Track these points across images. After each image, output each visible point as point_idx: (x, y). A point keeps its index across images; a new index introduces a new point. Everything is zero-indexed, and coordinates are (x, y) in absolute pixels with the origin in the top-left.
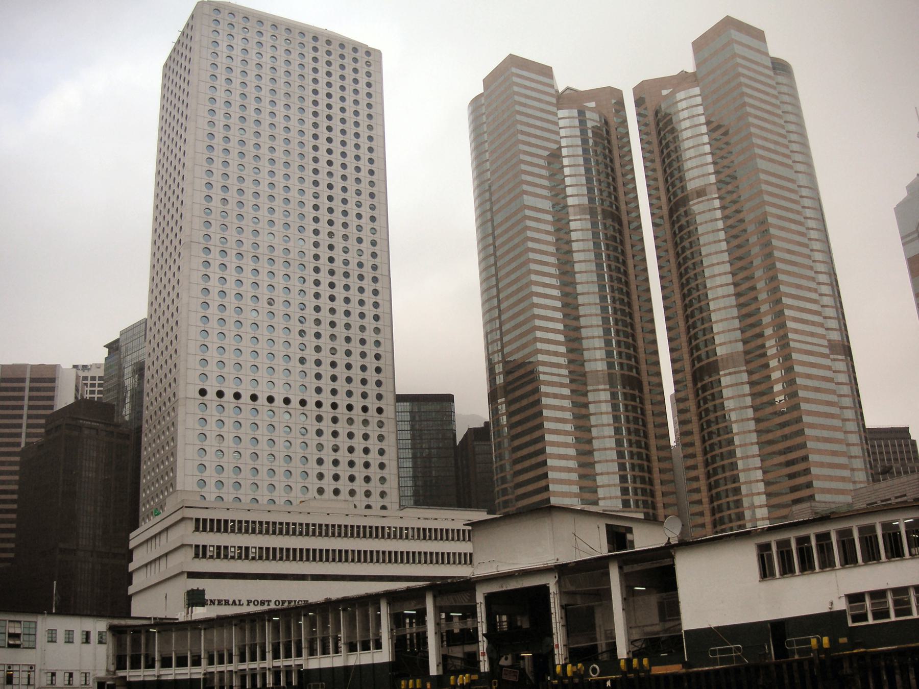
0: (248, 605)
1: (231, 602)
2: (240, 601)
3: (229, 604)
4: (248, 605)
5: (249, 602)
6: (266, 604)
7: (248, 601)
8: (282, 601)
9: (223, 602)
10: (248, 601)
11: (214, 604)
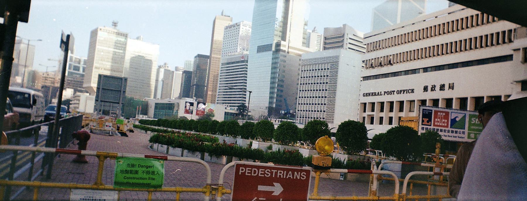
0: (384, 95)
1: (377, 94)
2: (381, 92)
3: (376, 95)
4: (384, 95)
5: (385, 92)
6: (393, 93)
7: (384, 92)
8: (400, 90)
9: (374, 94)
10: (384, 92)
11: (370, 96)
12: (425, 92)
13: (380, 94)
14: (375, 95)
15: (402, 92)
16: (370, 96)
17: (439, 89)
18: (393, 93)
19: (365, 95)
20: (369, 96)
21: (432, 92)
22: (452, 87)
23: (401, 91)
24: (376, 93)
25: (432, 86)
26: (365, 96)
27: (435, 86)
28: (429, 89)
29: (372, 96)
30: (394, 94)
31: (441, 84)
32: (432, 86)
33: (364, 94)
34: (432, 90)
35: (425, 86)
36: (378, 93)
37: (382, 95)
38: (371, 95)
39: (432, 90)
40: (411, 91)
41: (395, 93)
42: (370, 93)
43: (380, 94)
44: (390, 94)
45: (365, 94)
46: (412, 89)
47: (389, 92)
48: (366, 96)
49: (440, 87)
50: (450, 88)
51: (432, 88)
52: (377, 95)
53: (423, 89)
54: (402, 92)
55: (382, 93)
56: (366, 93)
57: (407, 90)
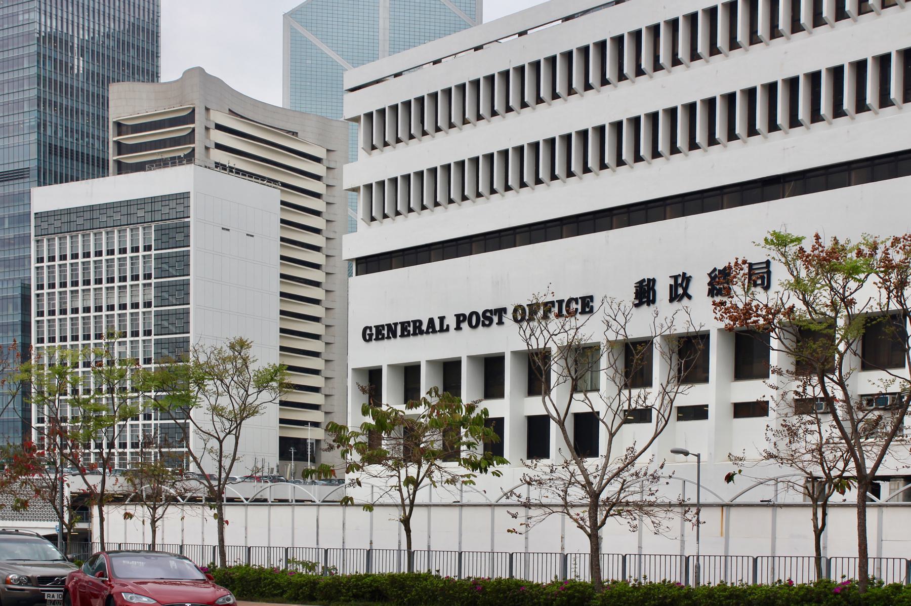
0: (458, 328)
1: (424, 327)
3: (422, 332)
4: (458, 328)
5: (460, 318)
6: (496, 319)
7: (458, 316)
9: (411, 329)
10: (458, 316)
12: (645, 306)
13: (438, 328)
14: (415, 334)
15: (541, 313)
16: (395, 336)
17: (707, 288)
18: (496, 319)
19: (371, 335)
20: (389, 338)
21: (675, 303)
22: (762, 278)
23: (534, 308)
24: (420, 322)
25: (676, 281)
26: (370, 340)
27: (687, 279)
28: (662, 291)
29: (402, 336)
30: (500, 322)
31: (715, 269)
32: (675, 278)
33: (368, 332)
34: (674, 297)
35: (644, 280)
36: (431, 321)
37: (448, 329)
38: (399, 333)
39: (674, 297)
40: (579, 307)
41: (508, 318)
42: (396, 324)
43: (438, 328)
44: (484, 325)
45: (370, 328)
46: (583, 299)
47: (476, 313)
48: (377, 339)
49: (708, 280)
50: (755, 285)
51: (673, 289)
52: (427, 332)
53: (634, 295)
54: (541, 313)
55: (446, 323)
56: (377, 327)
57: (560, 302)
